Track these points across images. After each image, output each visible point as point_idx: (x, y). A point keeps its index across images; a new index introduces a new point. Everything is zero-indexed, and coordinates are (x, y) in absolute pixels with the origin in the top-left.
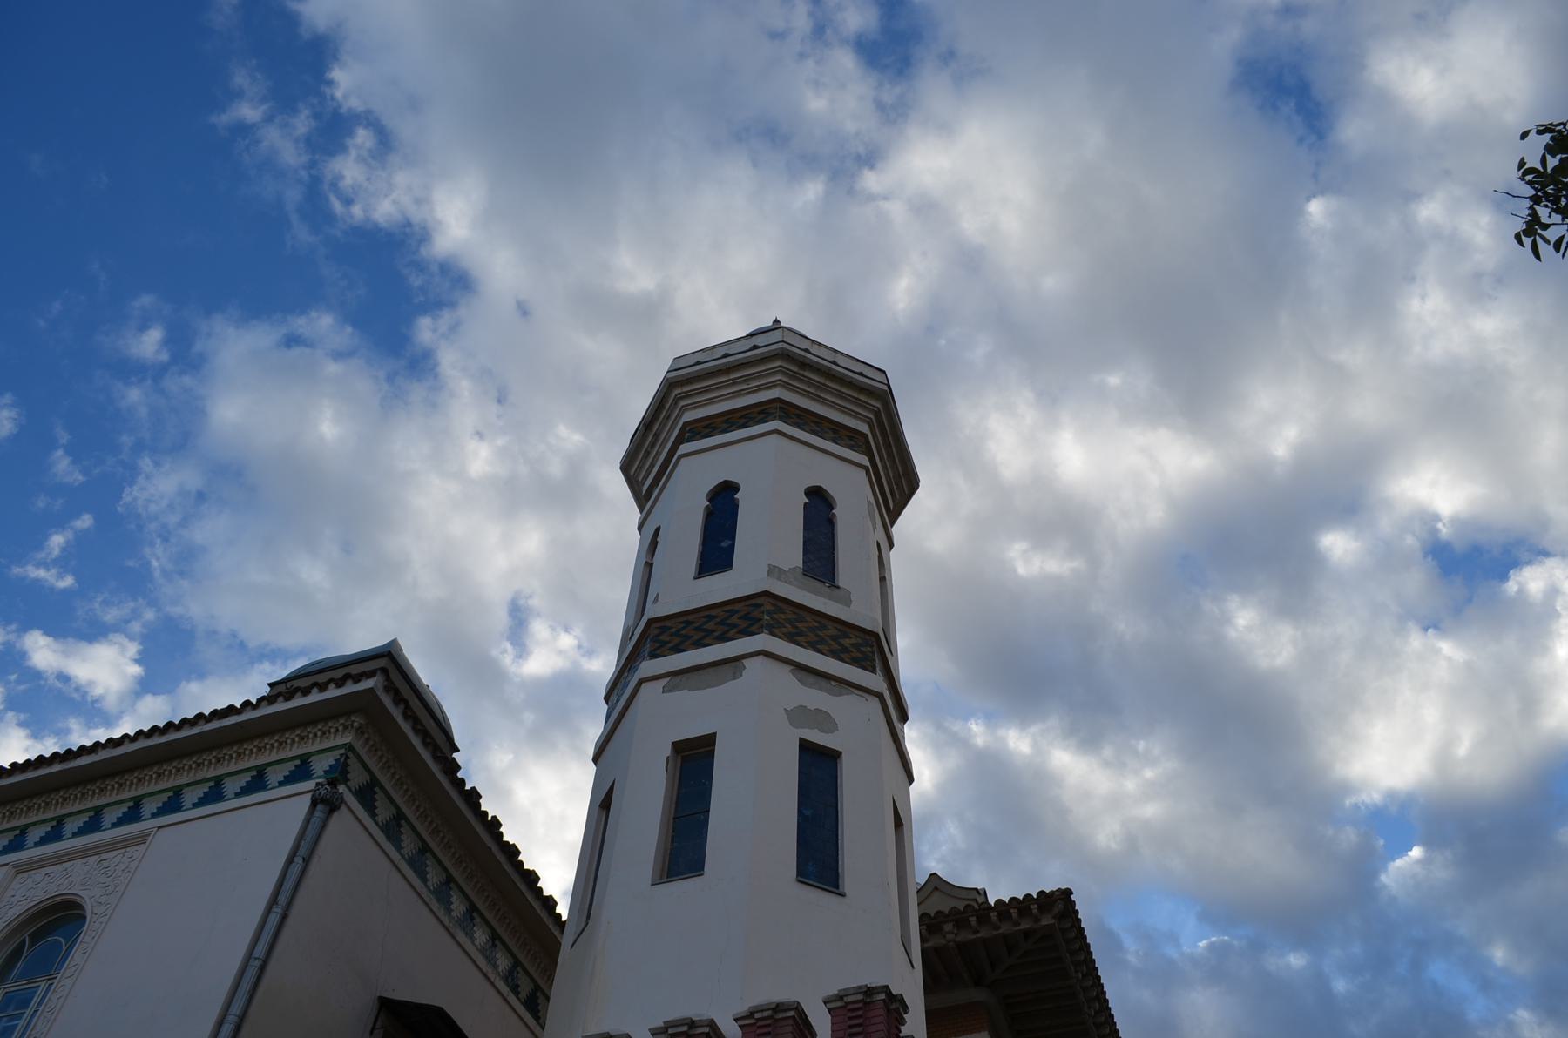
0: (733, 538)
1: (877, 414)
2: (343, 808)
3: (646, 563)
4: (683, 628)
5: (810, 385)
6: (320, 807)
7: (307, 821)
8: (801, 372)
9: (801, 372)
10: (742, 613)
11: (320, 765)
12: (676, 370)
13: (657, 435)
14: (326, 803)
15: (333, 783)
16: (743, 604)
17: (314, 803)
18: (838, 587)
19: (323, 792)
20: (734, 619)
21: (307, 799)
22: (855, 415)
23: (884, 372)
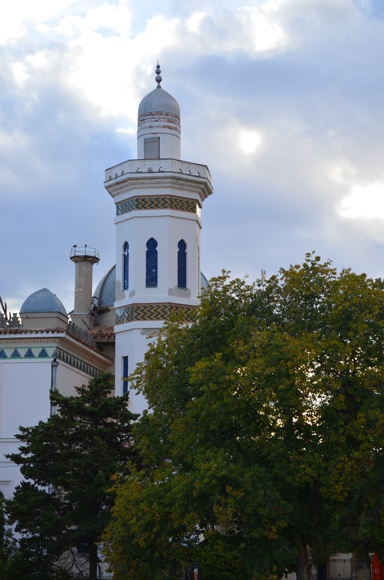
0: (156, 269)
1: (202, 190)
2: (59, 365)
3: (125, 255)
4: (144, 309)
5: (180, 185)
6: (54, 368)
7: (52, 372)
8: (178, 182)
9: (178, 182)
10: (162, 308)
11: (50, 351)
12: (132, 173)
13: (121, 188)
14: (54, 365)
15: (55, 360)
16: (161, 304)
17: (52, 366)
18: (187, 289)
19: (55, 364)
20: (159, 310)
21: (50, 365)
22: (194, 191)
23: (206, 166)
